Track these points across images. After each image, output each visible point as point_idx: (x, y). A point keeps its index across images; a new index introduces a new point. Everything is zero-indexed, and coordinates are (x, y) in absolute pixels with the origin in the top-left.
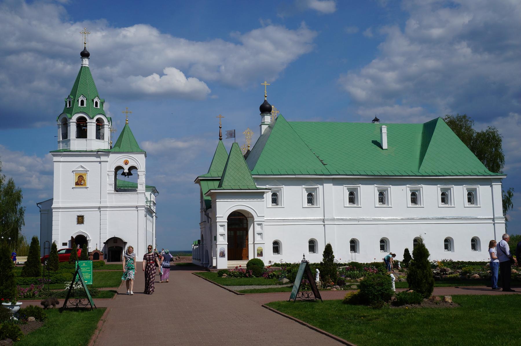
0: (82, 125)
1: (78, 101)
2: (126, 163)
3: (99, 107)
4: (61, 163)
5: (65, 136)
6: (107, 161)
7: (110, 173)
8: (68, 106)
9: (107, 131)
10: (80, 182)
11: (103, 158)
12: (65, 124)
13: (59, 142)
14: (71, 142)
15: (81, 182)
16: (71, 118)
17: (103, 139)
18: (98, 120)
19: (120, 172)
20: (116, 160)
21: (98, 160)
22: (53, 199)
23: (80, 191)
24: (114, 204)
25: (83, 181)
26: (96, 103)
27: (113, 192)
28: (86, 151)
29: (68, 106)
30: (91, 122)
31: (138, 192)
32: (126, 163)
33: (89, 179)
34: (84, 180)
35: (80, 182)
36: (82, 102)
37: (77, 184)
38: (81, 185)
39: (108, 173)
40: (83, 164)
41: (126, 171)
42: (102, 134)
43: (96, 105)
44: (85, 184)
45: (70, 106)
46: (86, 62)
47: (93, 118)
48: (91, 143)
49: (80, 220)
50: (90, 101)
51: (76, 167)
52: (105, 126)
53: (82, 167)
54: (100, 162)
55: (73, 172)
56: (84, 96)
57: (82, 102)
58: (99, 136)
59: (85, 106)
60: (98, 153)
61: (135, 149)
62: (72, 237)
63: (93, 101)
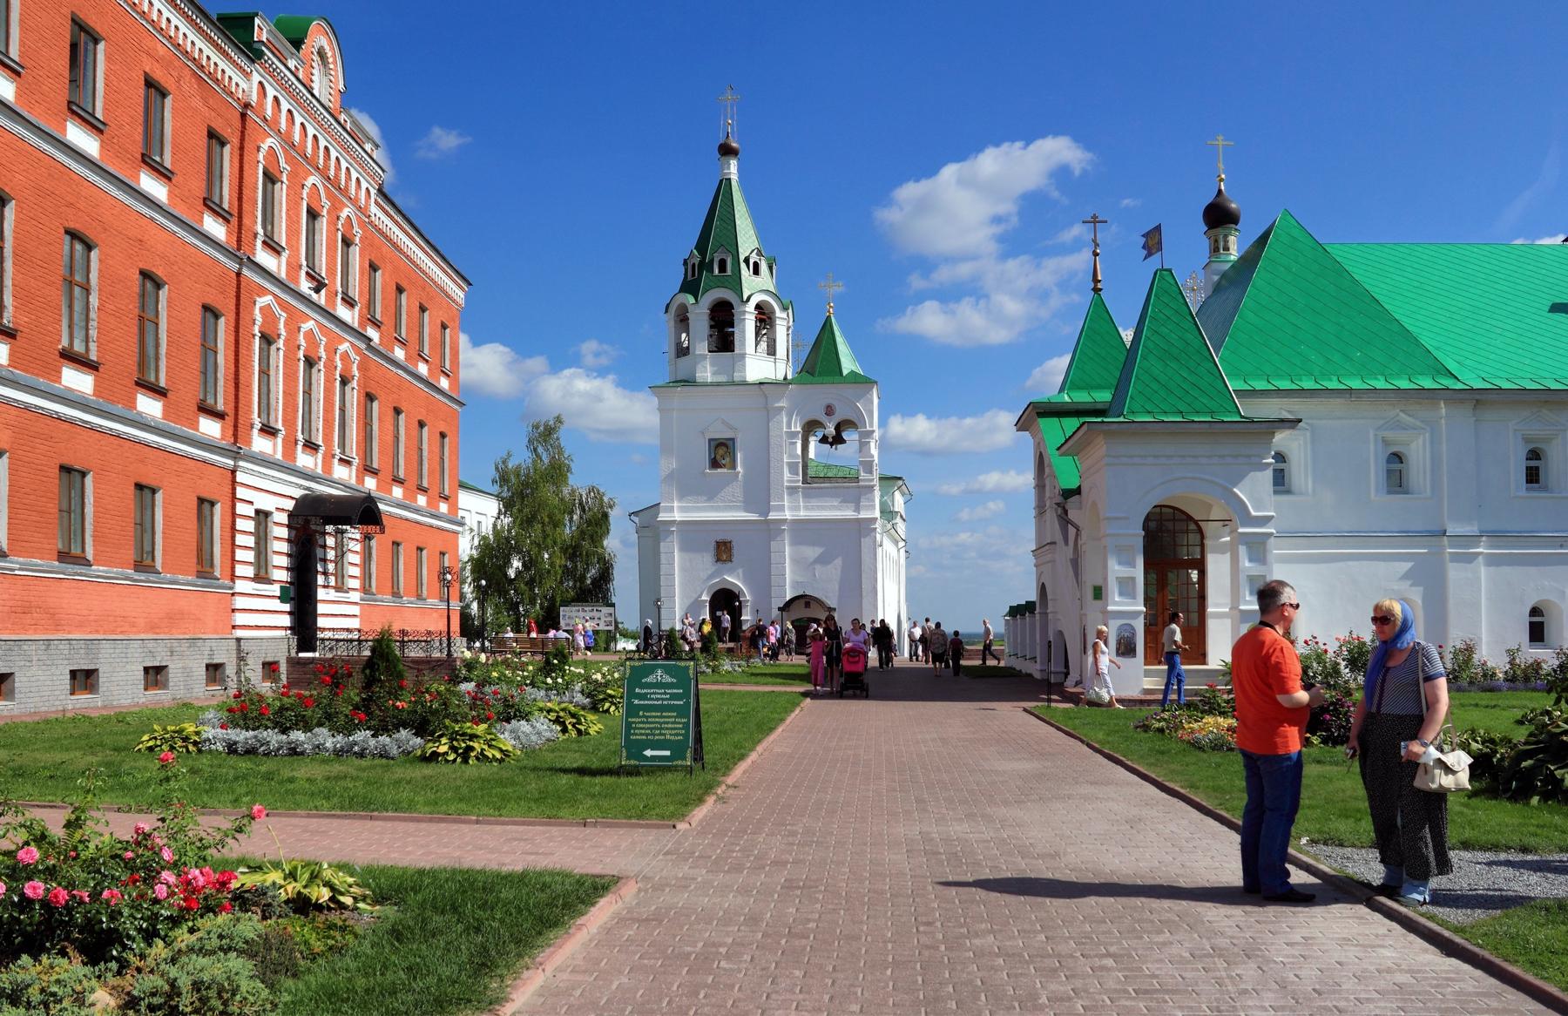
2: (829, 411)
32: (829, 411)
53: (724, 422)
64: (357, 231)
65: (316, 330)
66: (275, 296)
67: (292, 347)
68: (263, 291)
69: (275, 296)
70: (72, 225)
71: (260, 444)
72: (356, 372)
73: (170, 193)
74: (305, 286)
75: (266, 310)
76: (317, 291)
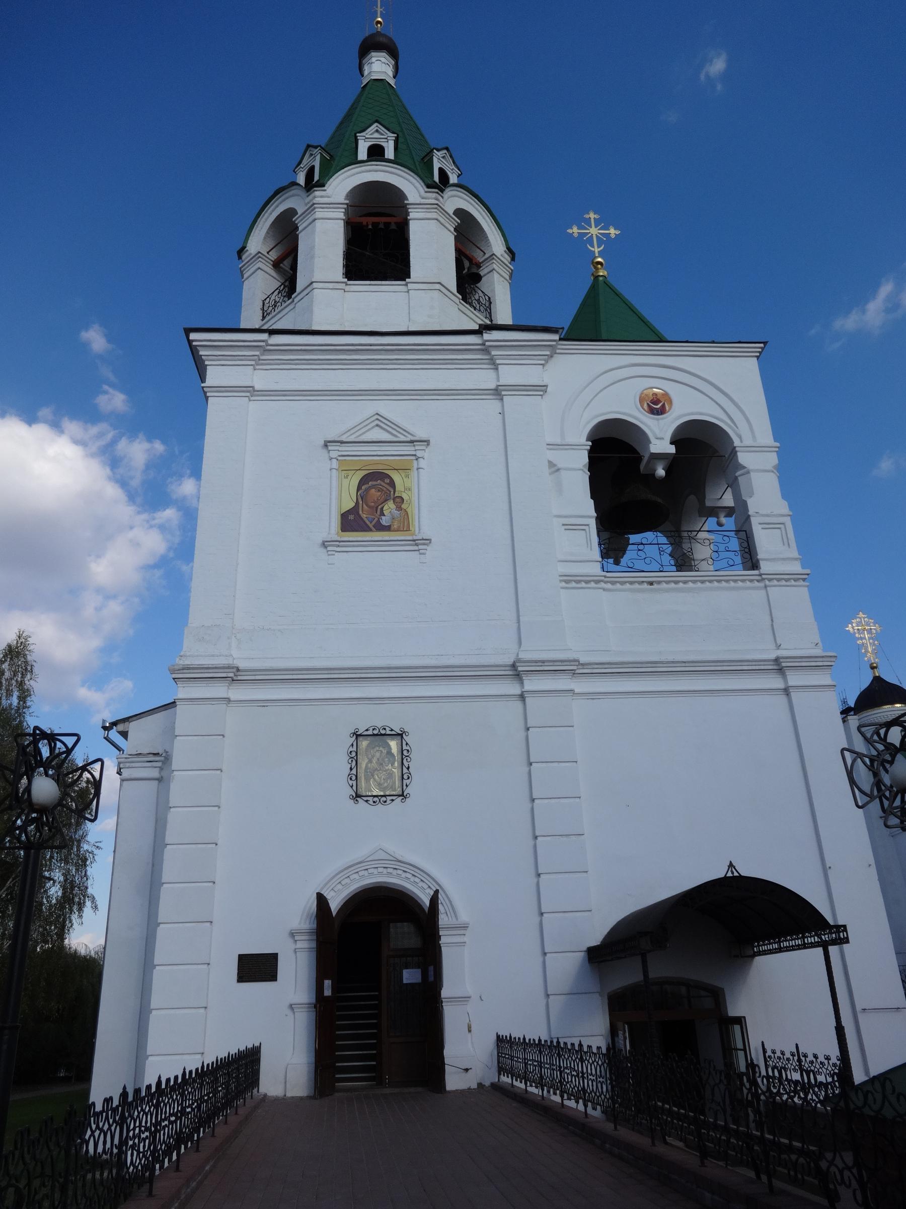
4: (255, 407)
6: (542, 389)
10: (374, 506)
21: (484, 378)
23: (372, 563)
24: (616, 648)
25: (389, 507)
31: (765, 567)
32: (657, 406)
35: (374, 506)
37: (351, 521)
38: (380, 528)
40: (391, 409)
44: (404, 525)
49: (379, 762)
51: (344, 418)
53: (380, 420)
54: (498, 393)
62: (321, 900)
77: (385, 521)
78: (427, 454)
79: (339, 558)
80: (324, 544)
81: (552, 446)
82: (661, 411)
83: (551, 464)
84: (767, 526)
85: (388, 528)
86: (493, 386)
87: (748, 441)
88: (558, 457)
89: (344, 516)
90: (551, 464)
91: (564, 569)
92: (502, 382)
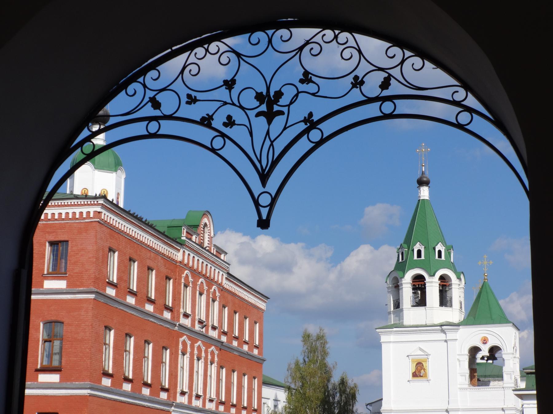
0: (419, 284)
1: (413, 250)
2: (485, 341)
3: (443, 258)
4: (391, 345)
5: (397, 305)
7: (461, 358)
8: (400, 260)
9: (457, 292)
10: (419, 372)
11: (450, 335)
12: (397, 286)
13: (390, 313)
14: (405, 312)
15: (420, 372)
16: (403, 277)
17: (451, 306)
18: (443, 278)
19: (479, 355)
20: (473, 335)
22: (382, 399)
23: (419, 383)
25: (422, 371)
26: (440, 252)
27: (467, 386)
28: (426, 326)
29: (400, 260)
30: (432, 282)
32: (485, 341)
33: (431, 367)
34: (424, 369)
35: (419, 372)
36: (419, 252)
37: (415, 375)
39: (458, 357)
41: (485, 352)
42: (448, 298)
43: (440, 256)
44: (425, 376)
45: (402, 259)
46: (425, 193)
47: (434, 275)
48: (434, 311)
50: (431, 250)
52: (453, 286)
53: (421, 349)
54: (446, 341)
55: (408, 356)
56: (444, 244)
57: (419, 252)
58: (444, 301)
59: (423, 257)
60: (443, 327)
61: (502, 319)
63: (434, 249)
64: (218, 294)
65: (201, 345)
66: (187, 335)
67: (192, 354)
68: (183, 335)
69: (187, 335)
70: (127, 332)
71: (180, 399)
72: (216, 359)
73: (154, 308)
74: (197, 327)
75: (184, 343)
76: (203, 328)
77: (421, 375)
78: (430, 357)
79: (412, 383)
80: (408, 381)
81: (459, 355)
82: (486, 343)
83: (458, 359)
84: (507, 374)
85: (422, 376)
86: (445, 339)
87: (505, 352)
88: (461, 358)
89: (413, 374)
90: (458, 359)
91: (459, 386)
92: (448, 338)
